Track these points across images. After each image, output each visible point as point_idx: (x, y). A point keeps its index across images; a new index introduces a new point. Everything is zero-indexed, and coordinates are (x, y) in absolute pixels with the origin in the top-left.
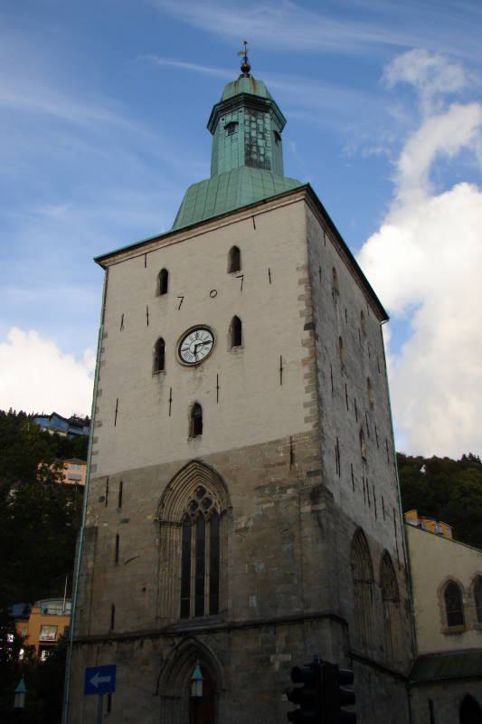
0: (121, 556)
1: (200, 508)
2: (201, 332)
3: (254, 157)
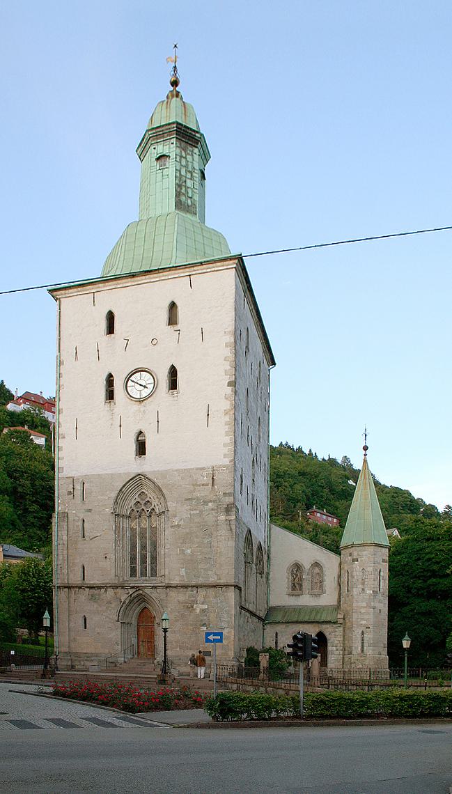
0: (86, 534)
3: (183, 199)
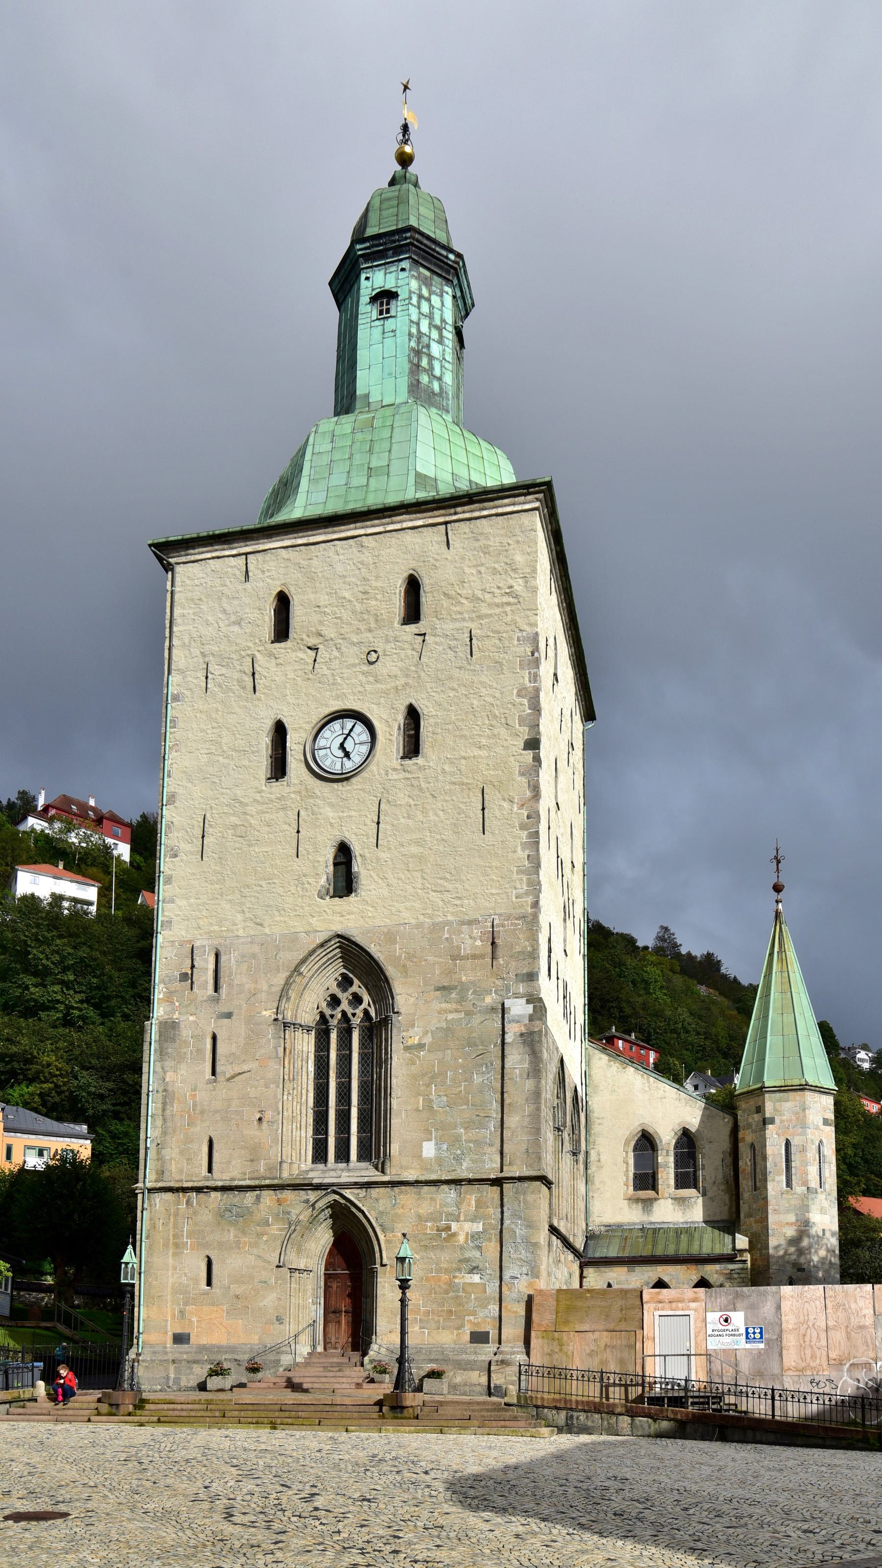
3: (424, 379)
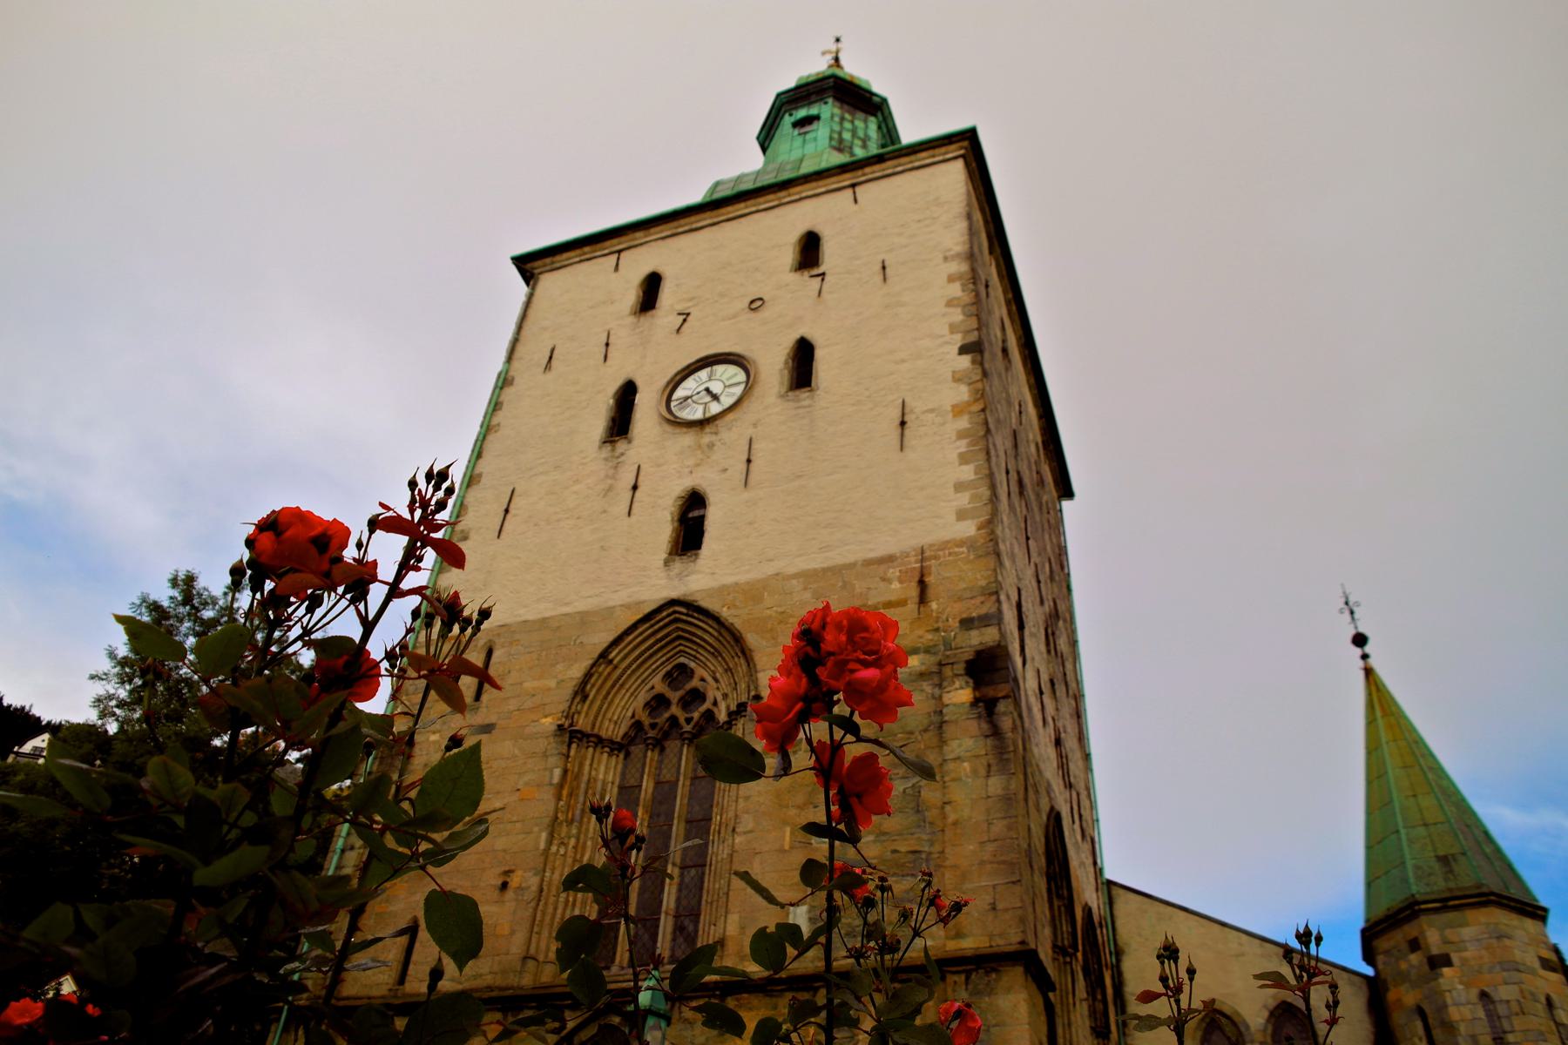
1: (675, 710)
2: (720, 369)
